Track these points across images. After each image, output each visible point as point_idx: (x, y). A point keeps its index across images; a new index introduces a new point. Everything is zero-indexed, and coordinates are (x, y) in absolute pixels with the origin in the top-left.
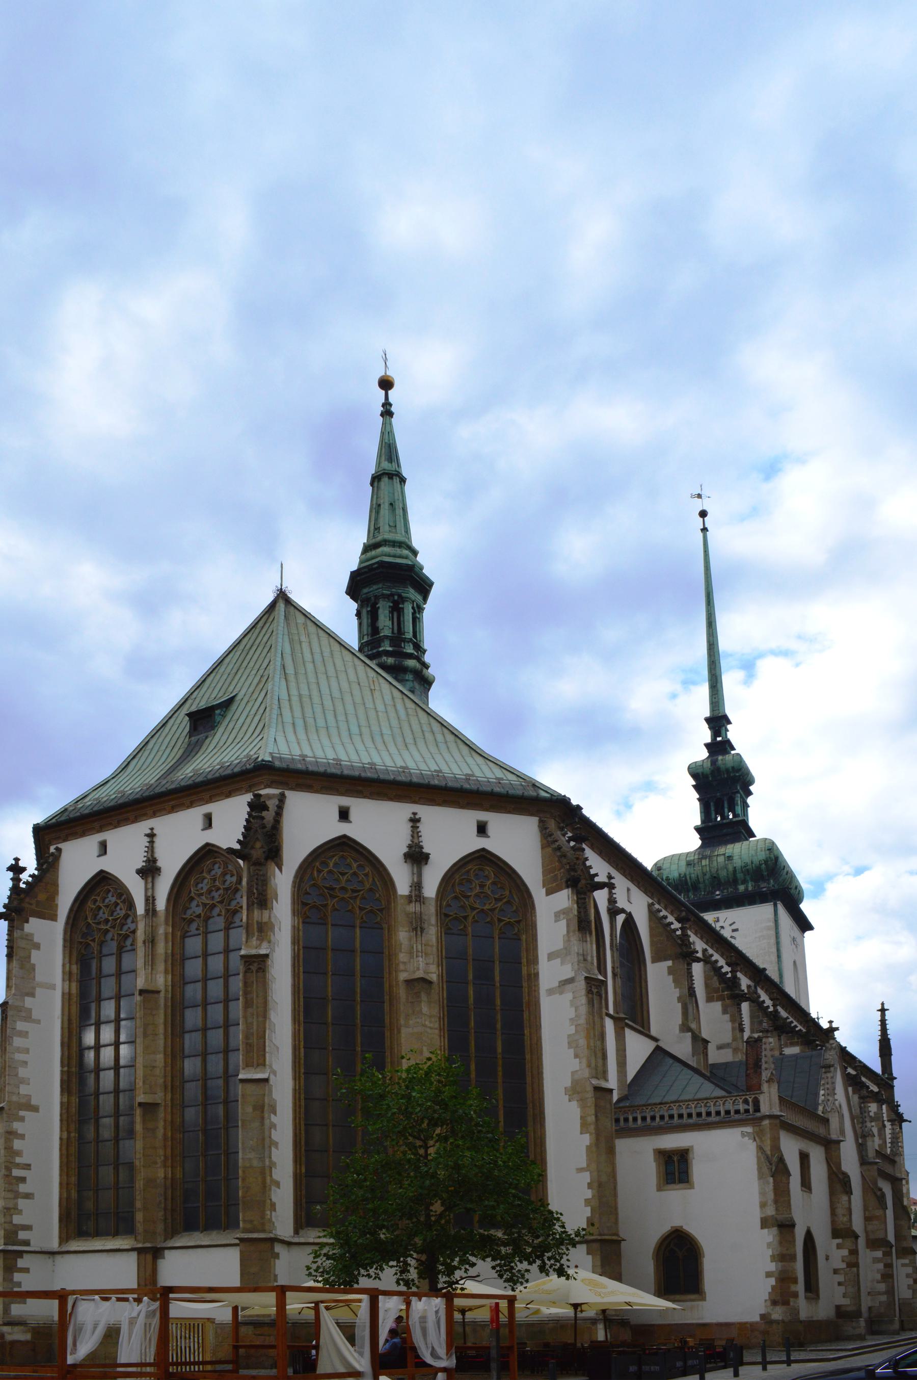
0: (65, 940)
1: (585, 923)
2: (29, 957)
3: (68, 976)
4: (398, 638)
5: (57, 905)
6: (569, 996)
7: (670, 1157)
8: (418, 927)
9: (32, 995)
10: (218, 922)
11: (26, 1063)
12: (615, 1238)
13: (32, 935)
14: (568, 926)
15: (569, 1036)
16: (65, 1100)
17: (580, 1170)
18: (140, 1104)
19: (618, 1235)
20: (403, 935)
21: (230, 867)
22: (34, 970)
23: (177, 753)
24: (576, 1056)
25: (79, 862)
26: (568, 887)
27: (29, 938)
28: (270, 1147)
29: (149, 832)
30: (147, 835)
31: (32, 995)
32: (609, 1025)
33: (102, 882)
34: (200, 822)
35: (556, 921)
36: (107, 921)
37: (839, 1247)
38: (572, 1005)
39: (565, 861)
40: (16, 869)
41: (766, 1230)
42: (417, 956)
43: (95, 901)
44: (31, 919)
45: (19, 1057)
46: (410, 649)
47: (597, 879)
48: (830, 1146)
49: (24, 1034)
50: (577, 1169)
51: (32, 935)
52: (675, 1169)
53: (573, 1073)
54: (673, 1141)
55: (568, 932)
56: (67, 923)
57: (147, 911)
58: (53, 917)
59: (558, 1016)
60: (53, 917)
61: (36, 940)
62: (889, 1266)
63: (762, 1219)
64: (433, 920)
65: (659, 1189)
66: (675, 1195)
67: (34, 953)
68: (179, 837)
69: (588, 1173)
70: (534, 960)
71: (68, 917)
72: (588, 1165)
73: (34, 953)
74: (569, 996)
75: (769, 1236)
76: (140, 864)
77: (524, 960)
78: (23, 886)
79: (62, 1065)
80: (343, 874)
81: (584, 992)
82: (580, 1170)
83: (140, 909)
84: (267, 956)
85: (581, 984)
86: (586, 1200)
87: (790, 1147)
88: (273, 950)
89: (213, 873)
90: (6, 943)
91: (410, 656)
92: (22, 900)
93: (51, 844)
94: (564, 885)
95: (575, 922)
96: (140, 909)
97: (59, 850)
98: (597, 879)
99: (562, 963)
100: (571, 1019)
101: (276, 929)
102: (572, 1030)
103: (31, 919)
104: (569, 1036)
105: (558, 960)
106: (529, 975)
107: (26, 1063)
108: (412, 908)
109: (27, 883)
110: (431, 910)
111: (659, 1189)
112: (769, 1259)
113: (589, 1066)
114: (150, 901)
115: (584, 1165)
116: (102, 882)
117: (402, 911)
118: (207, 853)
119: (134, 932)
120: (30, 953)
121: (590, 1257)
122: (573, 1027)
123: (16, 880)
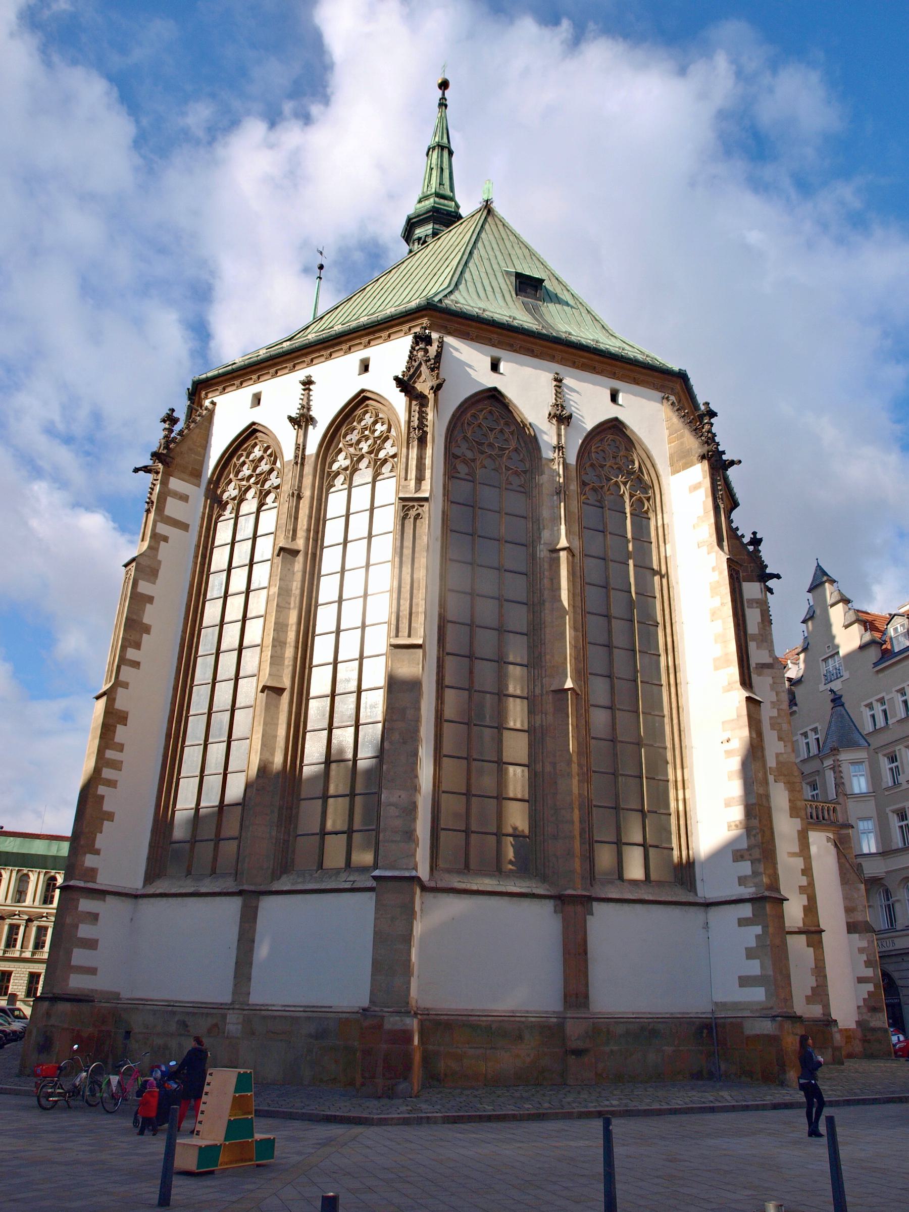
21: (381, 416)
33: (251, 433)
34: (356, 366)
68: (335, 381)
80: (491, 430)
89: (363, 423)
118: (361, 400)
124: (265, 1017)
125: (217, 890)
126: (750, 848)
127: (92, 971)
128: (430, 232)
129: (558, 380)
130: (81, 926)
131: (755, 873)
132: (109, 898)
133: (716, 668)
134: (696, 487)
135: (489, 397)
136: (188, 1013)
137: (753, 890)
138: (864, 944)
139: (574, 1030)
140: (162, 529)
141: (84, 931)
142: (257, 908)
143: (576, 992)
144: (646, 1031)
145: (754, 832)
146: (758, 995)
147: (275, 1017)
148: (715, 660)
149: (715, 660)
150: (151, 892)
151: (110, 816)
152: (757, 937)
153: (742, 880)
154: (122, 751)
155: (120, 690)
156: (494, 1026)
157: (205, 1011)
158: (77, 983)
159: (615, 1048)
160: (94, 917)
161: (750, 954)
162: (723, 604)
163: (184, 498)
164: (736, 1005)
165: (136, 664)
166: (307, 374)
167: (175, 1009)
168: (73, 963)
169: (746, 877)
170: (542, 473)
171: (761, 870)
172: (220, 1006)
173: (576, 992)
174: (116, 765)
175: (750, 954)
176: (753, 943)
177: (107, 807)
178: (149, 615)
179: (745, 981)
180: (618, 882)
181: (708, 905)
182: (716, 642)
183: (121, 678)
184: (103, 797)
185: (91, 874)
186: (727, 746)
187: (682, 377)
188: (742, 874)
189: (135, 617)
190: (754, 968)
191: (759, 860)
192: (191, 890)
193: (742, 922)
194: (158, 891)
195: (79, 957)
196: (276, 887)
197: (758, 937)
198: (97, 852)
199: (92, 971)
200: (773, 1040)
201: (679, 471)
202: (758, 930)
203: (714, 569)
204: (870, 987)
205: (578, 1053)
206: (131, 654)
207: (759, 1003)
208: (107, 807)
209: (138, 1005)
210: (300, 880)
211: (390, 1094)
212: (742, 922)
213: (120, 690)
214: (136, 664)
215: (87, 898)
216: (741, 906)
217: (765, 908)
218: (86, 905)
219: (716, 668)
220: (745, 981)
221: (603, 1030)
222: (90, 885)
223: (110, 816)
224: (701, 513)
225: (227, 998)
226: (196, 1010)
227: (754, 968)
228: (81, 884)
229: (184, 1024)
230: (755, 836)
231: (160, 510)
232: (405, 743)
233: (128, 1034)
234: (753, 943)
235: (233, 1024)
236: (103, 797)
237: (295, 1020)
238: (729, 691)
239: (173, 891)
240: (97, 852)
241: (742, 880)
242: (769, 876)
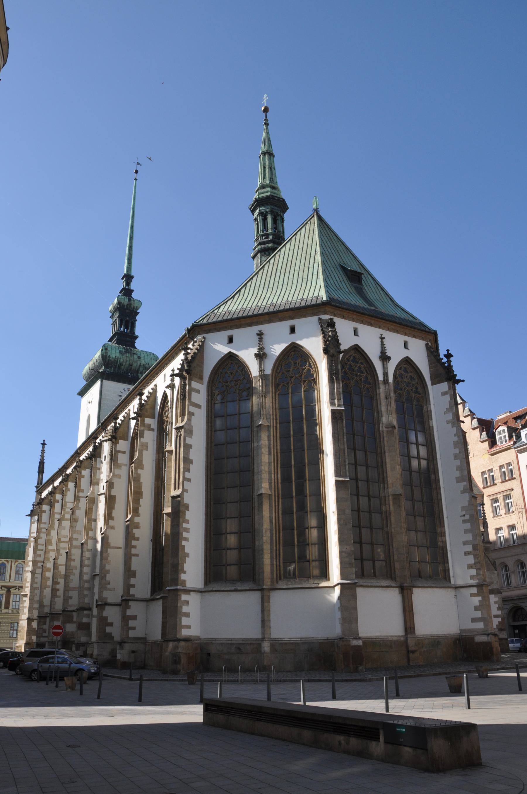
116: (231, 357)
124: (281, 643)
125: (247, 588)
126: (475, 564)
127: (189, 627)
128: (269, 210)
129: (382, 338)
130: (183, 607)
131: (478, 574)
132: (191, 593)
133: (458, 482)
134: (444, 394)
136: (240, 644)
137: (477, 581)
138: (497, 599)
139: (411, 643)
140: (192, 409)
141: (185, 609)
142: (269, 596)
143: (409, 626)
144: (435, 642)
145: (477, 556)
146: (480, 625)
147: (286, 644)
148: (456, 478)
149: (456, 478)
150: (210, 589)
151: (188, 555)
152: (479, 601)
153: (472, 577)
154: (188, 523)
155: (185, 493)
156: (381, 642)
157: (250, 642)
158: (185, 633)
159: (425, 650)
160: (187, 602)
161: (476, 608)
162: (460, 452)
163: (198, 391)
164: (470, 630)
165: (189, 480)
166: (260, 329)
167: (233, 642)
168: (183, 624)
169: (473, 576)
170: (379, 388)
171: (481, 572)
172: (257, 640)
173: (409, 626)
174: (187, 530)
175: (476, 608)
176: (477, 604)
177: (186, 551)
178: (192, 455)
179: (474, 620)
180: (420, 579)
181: (457, 588)
182: (457, 470)
183: (185, 488)
184: (184, 546)
185: (184, 582)
186: (463, 518)
187: (435, 334)
188: (472, 574)
189: (186, 456)
190: (478, 614)
191: (480, 569)
192: (233, 588)
193: (472, 595)
194: (214, 589)
195: (184, 621)
196: (278, 587)
197: (479, 601)
198: (185, 572)
199: (189, 627)
200: (489, 644)
201: (436, 384)
202: (480, 598)
203: (455, 435)
204: (500, 619)
205: (413, 652)
206: (187, 475)
207: (480, 629)
208: (186, 551)
209: (210, 642)
210: (290, 583)
211: (356, 670)
212: (472, 595)
213: (185, 493)
214: (189, 480)
215: (184, 594)
216: (471, 588)
217: (482, 589)
218: (184, 597)
219: (458, 482)
220: (474, 620)
221: (422, 641)
222: (184, 588)
223: (188, 555)
224: (448, 407)
225: (259, 636)
226: (244, 642)
227: (478, 614)
228: (181, 588)
229: (239, 649)
230: (477, 558)
231: (190, 399)
232: (346, 525)
233: (209, 654)
234: (477, 604)
235: (266, 647)
236: (184, 546)
237: (297, 644)
238: (464, 493)
239: (222, 589)
240: (185, 572)
241: (472, 577)
242: (483, 575)
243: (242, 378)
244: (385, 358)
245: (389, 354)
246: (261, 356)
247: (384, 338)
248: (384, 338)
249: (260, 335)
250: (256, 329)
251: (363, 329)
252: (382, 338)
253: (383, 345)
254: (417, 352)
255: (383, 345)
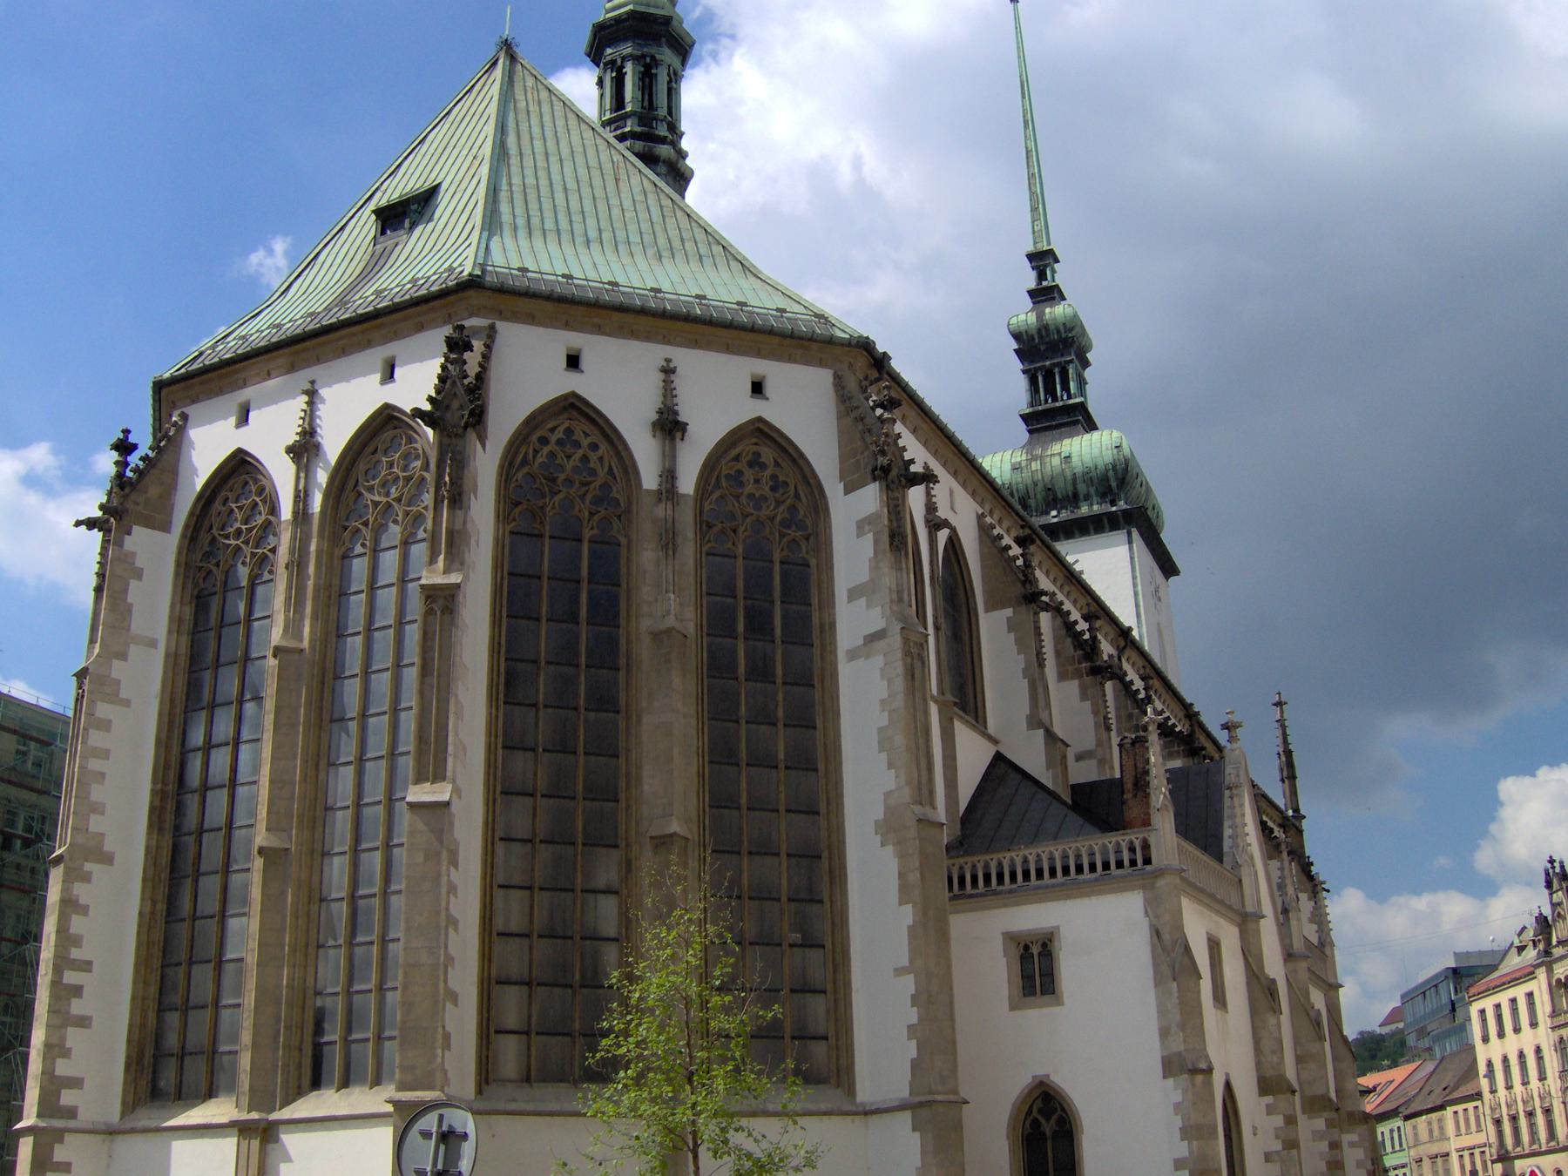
0: (178, 564)
1: (897, 538)
2: (126, 591)
3: (176, 621)
4: (647, 115)
5: (172, 507)
6: (878, 661)
7: (1026, 948)
8: (669, 542)
9: (123, 656)
10: (395, 532)
11: (103, 775)
12: (952, 1098)
13: (133, 554)
14: (876, 542)
15: (880, 730)
16: (154, 843)
17: (900, 971)
18: (261, 851)
19: (956, 1092)
20: (647, 556)
22: (130, 612)
23: (356, 268)
24: (890, 765)
25: (209, 444)
26: (874, 479)
27: (127, 559)
28: (447, 928)
29: (307, 386)
30: (306, 392)
31: (123, 656)
32: (934, 709)
33: (240, 466)
35: (858, 536)
36: (239, 533)
37: (1270, 1110)
38: (882, 677)
39: (869, 440)
40: (124, 447)
41: (1170, 1081)
42: (665, 599)
43: (226, 500)
44: (136, 529)
45: (94, 764)
46: (662, 131)
47: (913, 469)
48: (1246, 921)
49: (105, 725)
50: (896, 970)
51: (133, 554)
52: (1036, 969)
53: (887, 795)
54: (1031, 917)
55: (876, 552)
56: (184, 536)
57: (295, 513)
58: (165, 527)
59: (866, 695)
60: (165, 527)
61: (138, 564)
62: (1335, 1146)
63: (1163, 1058)
64: (690, 535)
65: (1013, 1007)
66: (1037, 1016)
67: (133, 583)
69: (912, 976)
70: (828, 602)
71: (187, 526)
72: (911, 961)
73: (133, 583)
74: (878, 661)
75: (1171, 1091)
76: (292, 438)
77: (815, 601)
78: (129, 474)
79: (154, 781)
81: (899, 655)
82: (900, 971)
83: (286, 512)
84: (458, 586)
85: (895, 640)
86: (909, 1027)
87: (1197, 925)
88: (466, 578)
90: (96, 567)
91: (663, 140)
92: (126, 497)
93: (174, 406)
94: (870, 476)
95: (885, 538)
96: (286, 512)
97: (185, 417)
98: (913, 469)
99: (868, 606)
100: (882, 701)
101: (473, 542)
102: (884, 720)
103: (136, 529)
104: (880, 730)
105: (863, 601)
106: (822, 625)
107: (103, 775)
108: (661, 511)
109: (136, 470)
110: (686, 518)
111: (1013, 1007)
112: (1178, 1135)
113: (909, 783)
114: (302, 498)
115: (905, 962)
116: (240, 466)
117: (648, 517)
118: (386, 420)
119: (273, 551)
120: (127, 585)
121: (917, 1134)
122: (886, 714)
123: (122, 465)
129: (668, 371)
135: (565, 409)
243: (260, 520)
244: (669, 426)
245: (683, 417)
246: (304, 449)
247: (673, 371)
248: (673, 371)
249: (312, 394)
250: (303, 377)
251: (596, 348)
252: (668, 371)
253: (668, 391)
254: (804, 408)
255: (668, 391)
